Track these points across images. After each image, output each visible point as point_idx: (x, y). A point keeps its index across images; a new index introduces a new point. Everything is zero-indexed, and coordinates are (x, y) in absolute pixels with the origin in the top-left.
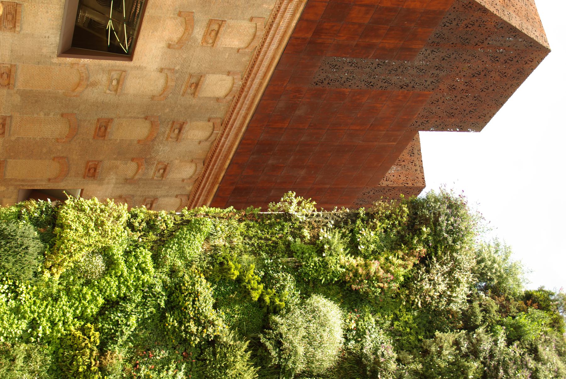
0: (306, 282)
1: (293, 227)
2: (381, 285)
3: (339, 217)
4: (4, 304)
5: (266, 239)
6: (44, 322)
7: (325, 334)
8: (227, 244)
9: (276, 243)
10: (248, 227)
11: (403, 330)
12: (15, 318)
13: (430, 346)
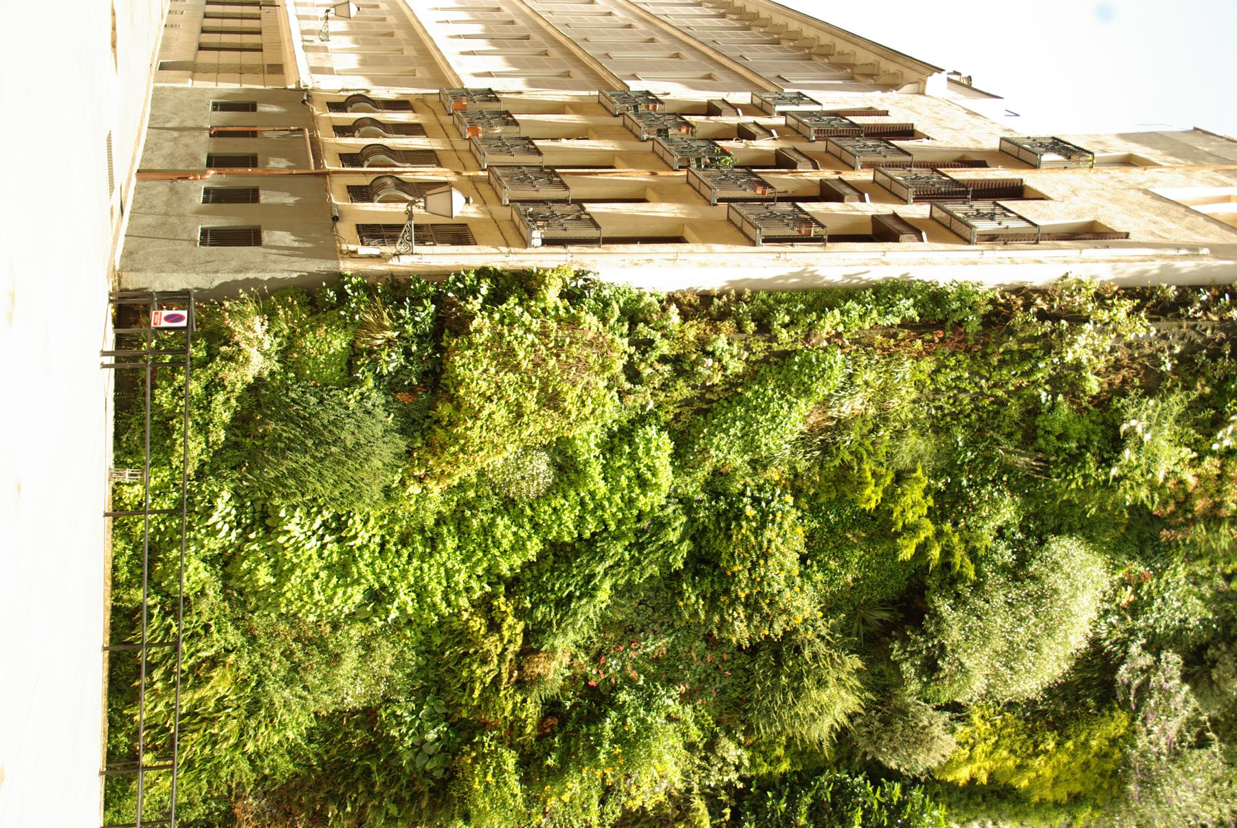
4: (315, 556)
6: (405, 598)
9: (1002, 403)
12: (337, 586)
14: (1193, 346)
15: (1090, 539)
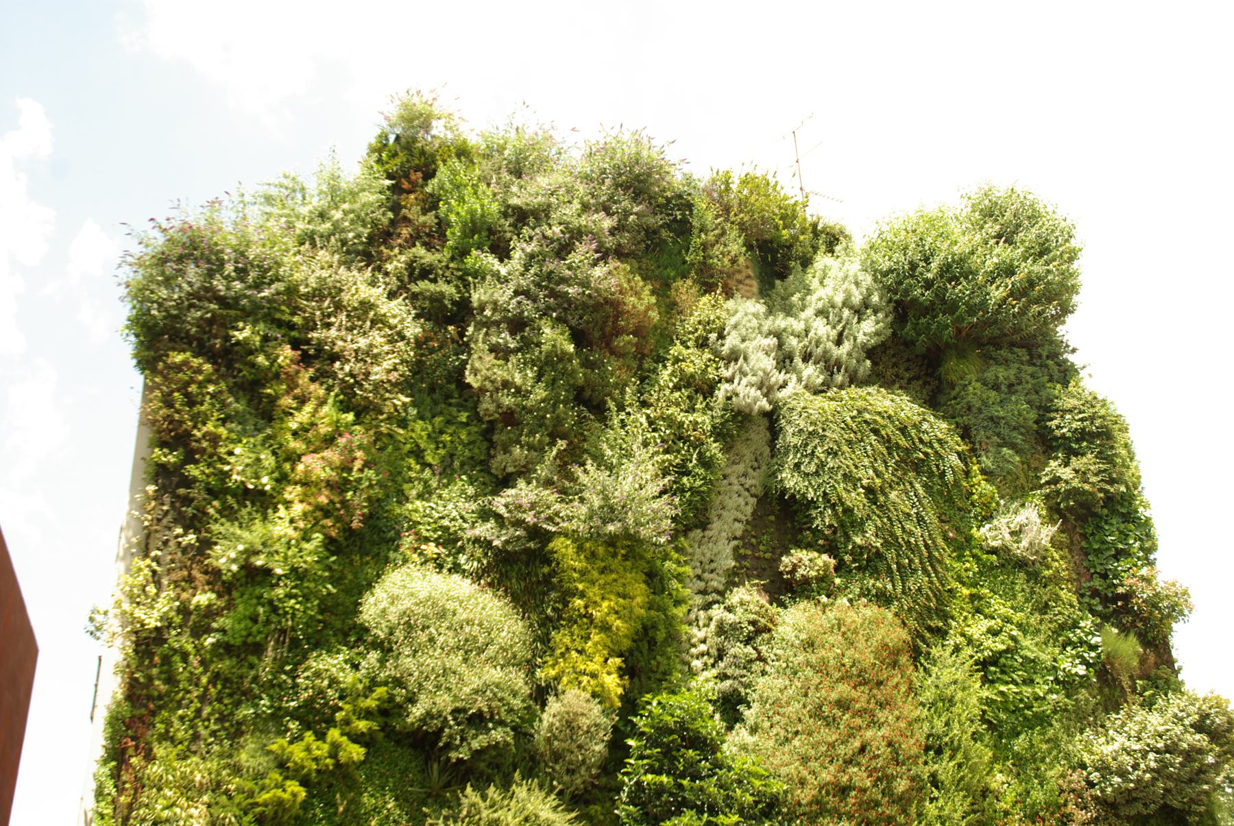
0: (325, 627)
1: (180, 627)
2: (358, 465)
3: (166, 513)
5: (203, 698)
7: (462, 615)
8: (205, 798)
10: (166, 737)
11: (444, 447)
13: (499, 406)
14: (180, 519)
15: (370, 586)
